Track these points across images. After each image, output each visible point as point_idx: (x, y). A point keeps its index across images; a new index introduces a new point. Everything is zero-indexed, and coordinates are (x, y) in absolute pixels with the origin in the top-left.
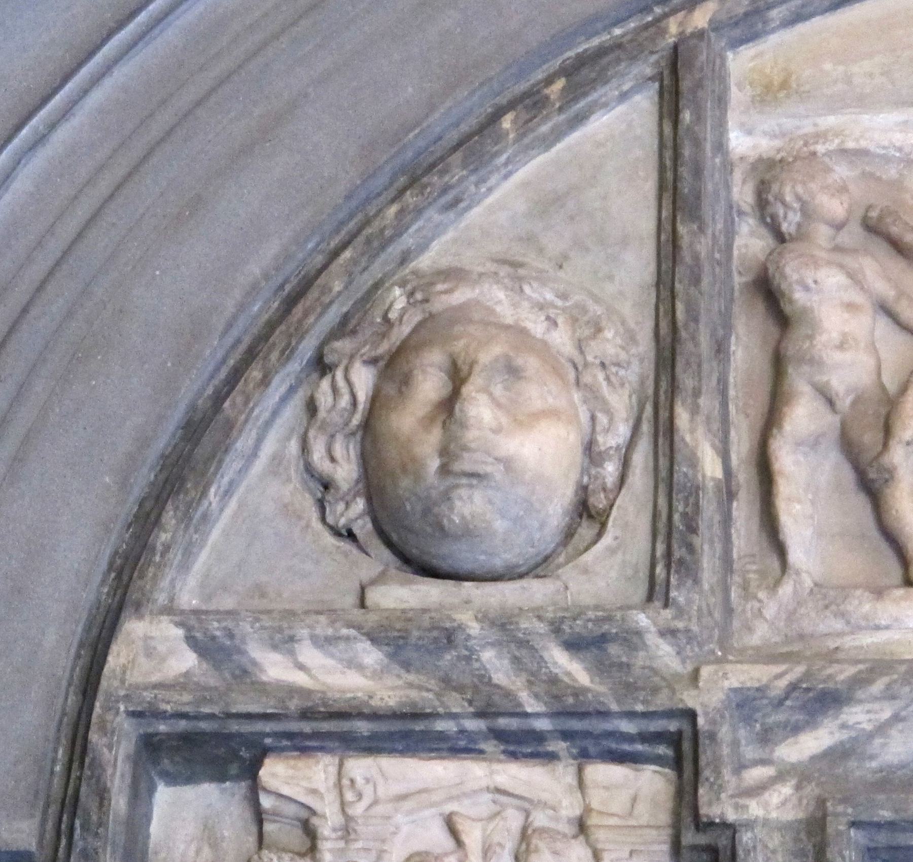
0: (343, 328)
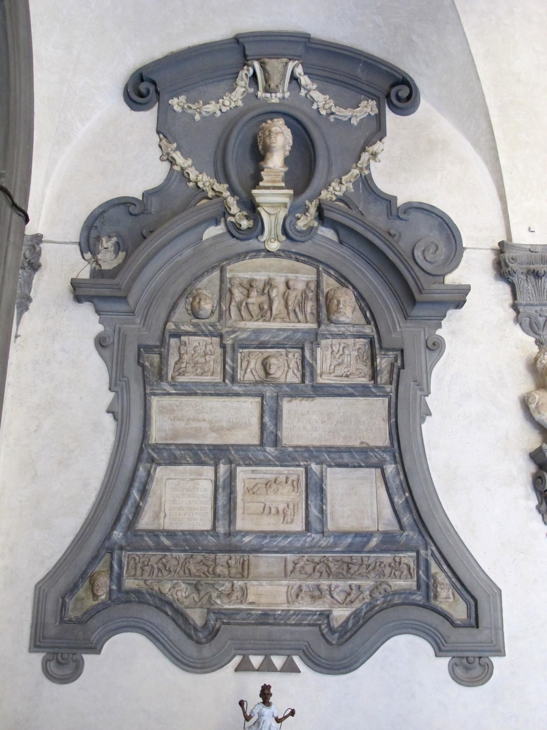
0: (189, 294)
